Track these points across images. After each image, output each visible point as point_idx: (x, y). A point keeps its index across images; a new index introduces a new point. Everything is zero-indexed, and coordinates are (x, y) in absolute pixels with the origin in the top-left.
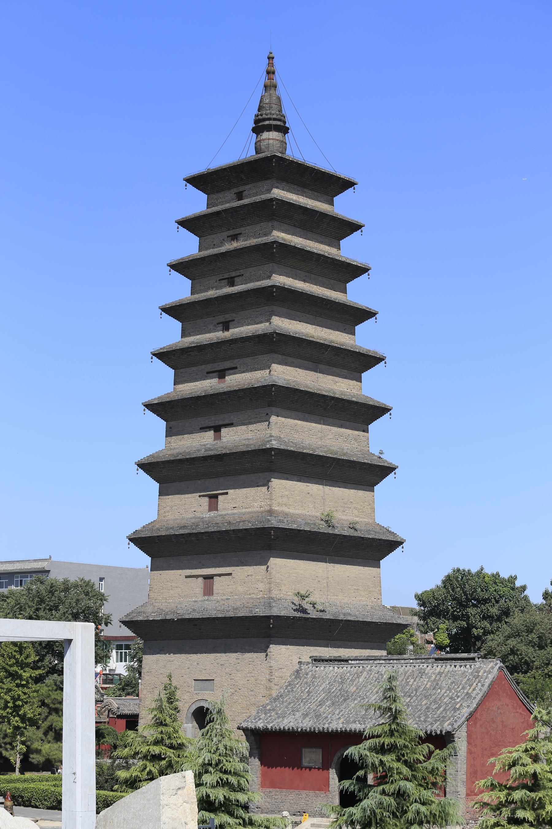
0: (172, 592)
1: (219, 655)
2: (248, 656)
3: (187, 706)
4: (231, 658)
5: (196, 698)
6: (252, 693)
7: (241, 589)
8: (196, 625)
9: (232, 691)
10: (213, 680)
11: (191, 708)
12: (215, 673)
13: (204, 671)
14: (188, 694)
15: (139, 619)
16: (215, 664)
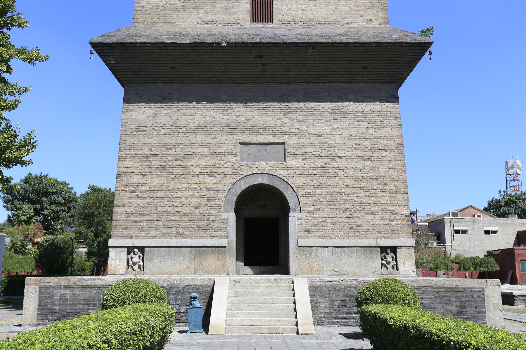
0: (185, 15)
1: (293, 106)
2: (368, 107)
3: (228, 183)
4: (322, 110)
5: (246, 171)
6: (366, 163)
7: (330, 16)
8: (261, 57)
9: (325, 160)
10: (284, 144)
11: (236, 187)
12: (287, 133)
13: (261, 131)
14: (229, 165)
15: (138, 41)
16: (287, 121)
